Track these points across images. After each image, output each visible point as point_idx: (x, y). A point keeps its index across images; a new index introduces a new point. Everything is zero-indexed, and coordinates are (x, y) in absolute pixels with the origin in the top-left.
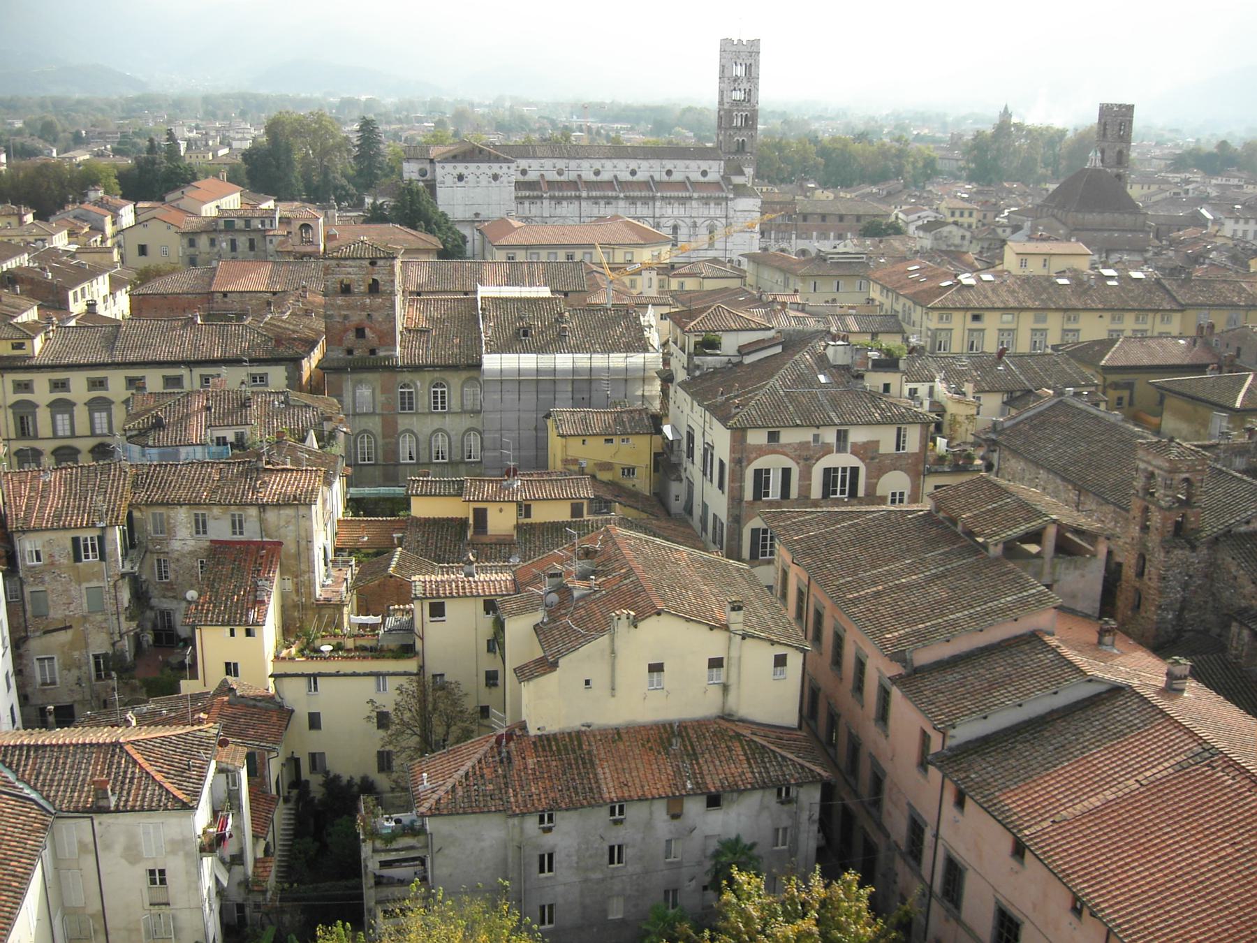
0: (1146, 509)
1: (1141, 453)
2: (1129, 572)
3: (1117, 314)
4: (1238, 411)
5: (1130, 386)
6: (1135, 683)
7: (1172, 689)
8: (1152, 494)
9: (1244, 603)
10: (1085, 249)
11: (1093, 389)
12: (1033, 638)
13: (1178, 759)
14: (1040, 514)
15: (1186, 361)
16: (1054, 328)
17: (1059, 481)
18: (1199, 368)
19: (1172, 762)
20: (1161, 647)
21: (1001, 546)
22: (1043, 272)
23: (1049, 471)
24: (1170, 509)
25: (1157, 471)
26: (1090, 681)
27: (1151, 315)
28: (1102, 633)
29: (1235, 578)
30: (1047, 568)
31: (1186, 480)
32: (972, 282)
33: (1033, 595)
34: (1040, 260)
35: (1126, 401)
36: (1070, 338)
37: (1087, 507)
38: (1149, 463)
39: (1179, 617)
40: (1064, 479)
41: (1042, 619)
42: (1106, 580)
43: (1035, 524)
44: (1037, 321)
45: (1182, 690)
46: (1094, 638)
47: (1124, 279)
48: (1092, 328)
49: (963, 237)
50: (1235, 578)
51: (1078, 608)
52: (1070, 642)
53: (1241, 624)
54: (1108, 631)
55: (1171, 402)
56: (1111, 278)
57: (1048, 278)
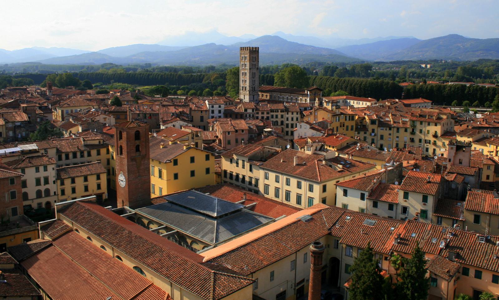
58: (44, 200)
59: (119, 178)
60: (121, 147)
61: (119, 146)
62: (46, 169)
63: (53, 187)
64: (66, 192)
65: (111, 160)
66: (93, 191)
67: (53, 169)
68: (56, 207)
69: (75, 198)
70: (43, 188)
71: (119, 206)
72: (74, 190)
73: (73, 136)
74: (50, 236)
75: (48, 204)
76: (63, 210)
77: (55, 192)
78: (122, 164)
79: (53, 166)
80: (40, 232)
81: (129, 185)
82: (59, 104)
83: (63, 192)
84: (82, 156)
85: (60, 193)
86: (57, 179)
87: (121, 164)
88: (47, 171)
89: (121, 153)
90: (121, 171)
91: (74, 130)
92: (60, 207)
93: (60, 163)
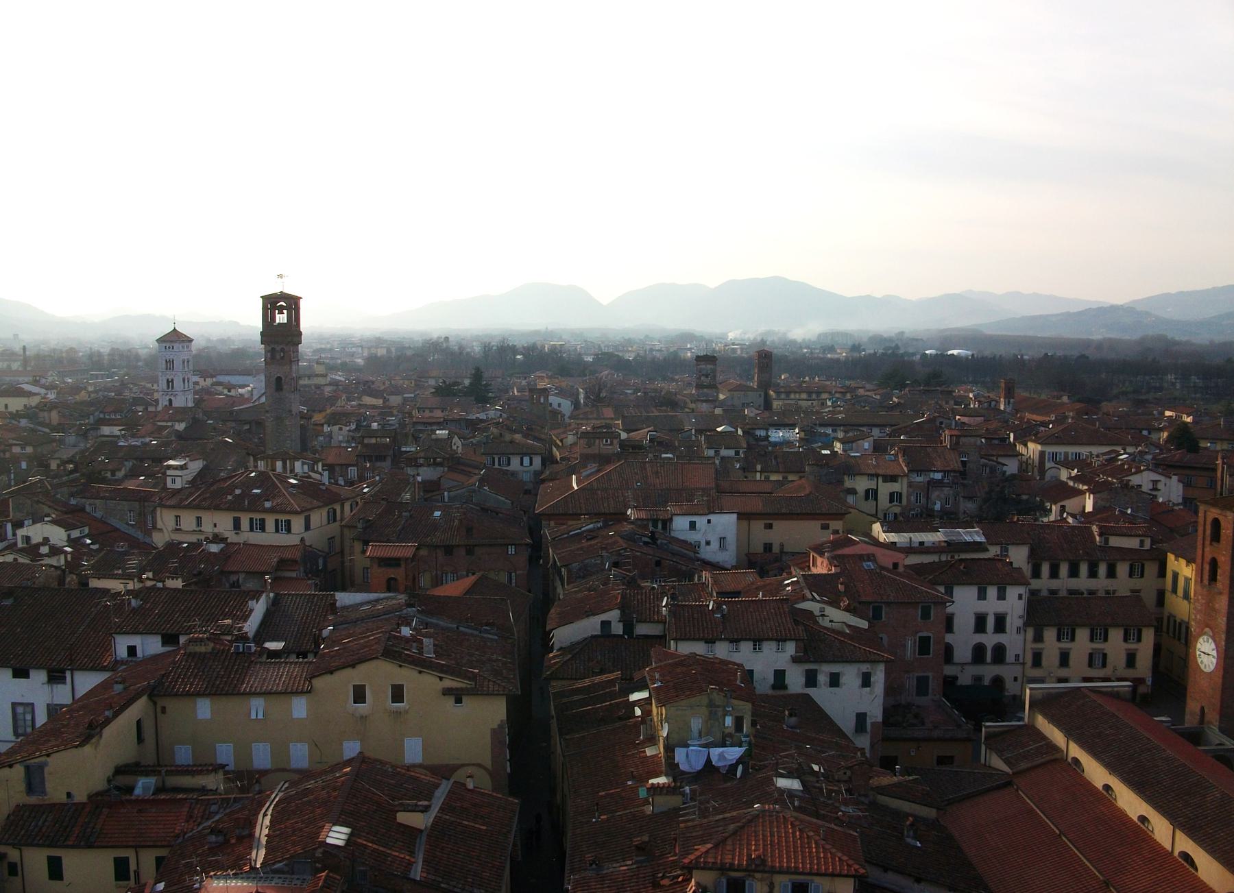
58: (989, 672)
59: (1199, 646)
60: (1214, 564)
61: (1208, 557)
62: (1001, 596)
63: (1015, 641)
64: (1044, 662)
65: (1169, 596)
66: (1115, 669)
67: (1020, 597)
68: (1028, 691)
69: (1065, 680)
70: (990, 639)
71: (1190, 721)
72: (1064, 659)
73: (1070, 520)
74: (1007, 762)
75: (998, 681)
76: (1044, 704)
77: (1017, 656)
78: (1214, 610)
79: (1021, 590)
80: (983, 747)
81: (1225, 669)
82: (1035, 435)
83: (1037, 660)
84: (1093, 574)
85: (1029, 659)
86: (1026, 625)
87: (1209, 609)
88: (1004, 599)
89: (1213, 578)
90: (1207, 626)
91: (1071, 504)
92: (1039, 694)
93: (1035, 584)
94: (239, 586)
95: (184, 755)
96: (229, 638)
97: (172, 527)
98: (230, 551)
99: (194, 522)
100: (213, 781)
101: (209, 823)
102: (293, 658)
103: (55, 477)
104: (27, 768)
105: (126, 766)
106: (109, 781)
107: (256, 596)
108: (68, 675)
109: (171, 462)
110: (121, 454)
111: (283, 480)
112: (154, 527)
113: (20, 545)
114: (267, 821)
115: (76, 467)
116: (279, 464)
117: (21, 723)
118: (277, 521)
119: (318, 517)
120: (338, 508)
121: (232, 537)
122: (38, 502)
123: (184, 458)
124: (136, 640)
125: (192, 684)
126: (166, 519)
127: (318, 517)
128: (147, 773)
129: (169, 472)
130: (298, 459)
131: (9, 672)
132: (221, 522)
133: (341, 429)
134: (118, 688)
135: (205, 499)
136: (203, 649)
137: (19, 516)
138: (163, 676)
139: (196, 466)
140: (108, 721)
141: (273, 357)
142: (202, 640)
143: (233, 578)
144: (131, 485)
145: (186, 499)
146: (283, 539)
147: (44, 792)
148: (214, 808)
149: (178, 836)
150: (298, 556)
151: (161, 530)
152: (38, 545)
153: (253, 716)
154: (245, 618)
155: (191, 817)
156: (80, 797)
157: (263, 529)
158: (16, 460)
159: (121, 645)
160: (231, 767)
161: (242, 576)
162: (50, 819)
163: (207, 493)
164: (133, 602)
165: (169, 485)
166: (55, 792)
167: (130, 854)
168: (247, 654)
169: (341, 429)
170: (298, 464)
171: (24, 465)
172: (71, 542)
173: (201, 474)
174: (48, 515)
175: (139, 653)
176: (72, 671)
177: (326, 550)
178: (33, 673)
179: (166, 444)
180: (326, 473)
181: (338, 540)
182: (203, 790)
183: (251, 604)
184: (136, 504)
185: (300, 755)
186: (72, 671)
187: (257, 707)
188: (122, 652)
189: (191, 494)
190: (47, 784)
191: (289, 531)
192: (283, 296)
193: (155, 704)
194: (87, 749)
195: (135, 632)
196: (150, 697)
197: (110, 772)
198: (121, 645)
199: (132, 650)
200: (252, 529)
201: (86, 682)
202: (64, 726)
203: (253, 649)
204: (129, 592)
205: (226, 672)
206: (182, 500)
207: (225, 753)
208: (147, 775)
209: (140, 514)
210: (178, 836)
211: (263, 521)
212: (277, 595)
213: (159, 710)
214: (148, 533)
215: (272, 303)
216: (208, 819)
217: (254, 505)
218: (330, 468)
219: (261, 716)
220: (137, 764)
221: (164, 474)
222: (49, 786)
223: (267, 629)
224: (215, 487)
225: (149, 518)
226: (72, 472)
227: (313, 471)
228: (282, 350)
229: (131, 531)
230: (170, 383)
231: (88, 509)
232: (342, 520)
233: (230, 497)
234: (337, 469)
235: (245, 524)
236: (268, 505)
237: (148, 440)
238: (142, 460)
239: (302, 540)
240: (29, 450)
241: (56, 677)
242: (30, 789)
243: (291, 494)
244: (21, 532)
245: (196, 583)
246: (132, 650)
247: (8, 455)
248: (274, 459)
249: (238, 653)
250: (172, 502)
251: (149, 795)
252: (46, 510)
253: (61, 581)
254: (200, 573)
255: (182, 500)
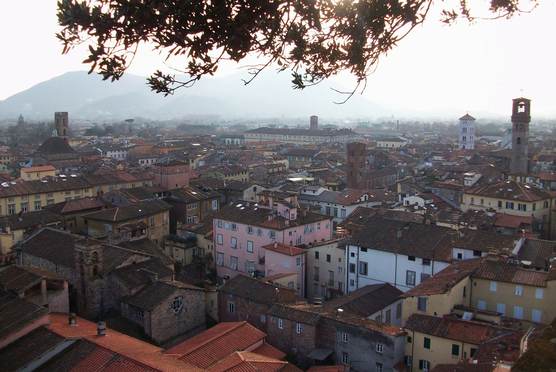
0: (82, 266)
1: (76, 245)
2: (80, 292)
3: (68, 192)
4: (115, 222)
5: (74, 219)
6: (85, 336)
7: (100, 334)
8: (83, 260)
9: (124, 295)
10: (53, 168)
11: (60, 222)
12: (43, 329)
13: (106, 362)
14: (38, 277)
15: (94, 206)
16: (44, 200)
17: (48, 261)
18: (99, 208)
19: (104, 364)
20: (96, 320)
21: (23, 294)
22: (38, 179)
23: (43, 258)
24: (90, 264)
25: (83, 251)
26: (67, 340)
27: (81, 191)
28: (70, 320)
29: (119, 286)
30: (45, 298)
31: (95, 252)
32: (7, 185)
33: (39, 311)
34: (36, 174)
35: (74, 224)
36: (51, 203)
37: (60, 270)
38: (79, 248)
39: (102, 305)
40: (49, 260)
41: (45, 320)
42: (70, 297)
43: (37, 282)
44: (36, 198)
45: (105, 334)
46: (68, 322)
47: (69, 178)
48: (59, 198)
49: (4, 168)
50: (119, 286)
51: (61, 311)
52: (58, 326)
53: (124, 302)
54: (73, 318)
55: (90, 222)
56: (64, 178)
57: (39, 181)
94: (501, 233)
95: (482, 305)
96: (507, 256)
97: (468, 203)
98: (497, 217)
99: (480, 201)
100: (497, 320)
101: (496, 338)
102: (534, 270)
103: (417, 176)
104: (419, 299)
105: (458, 305)
106: (451, 311)
107: (518, 239)
108: (431, 262)
109: (467, 174)
110: (443, 169)
111: (523, 186)
112: (462, 202)
113: (404, 204)
114: (526, 343)
115: (425, 173)
116: (518, 178)
117: (409, 279)
118: (519, 205)
119: (539, 205)
120: (549, 201)
121: (498, 211)
122: (412, 187)
123: (473, 172)
124: (462, 251)
125: (489, 275)
126: (467, 199)
127: (539, 205)
128: (468, 311)
129: (465, 178)
130: (528, 176)
131: (407, 257)
132: (493, 203)
133: (545, 163)
134: (456, 271)
135: (485, 192)
136: (494, 260)
137: (404, 192)
138: (476, 269)
139: (478, 176)
140: (453, 285)
141: (517, 128)
142: (494, 256)
143: (499, 229)
144: (447, 182)
145: (477, 191)
146: (521, 213)
147: (425, 310)
148: (499, 332)
149: (482, 341)
150: (530, 222)
151: (464, 203)
152: (413, 206)
153: (516, 294)
154: (513, 248)
155: (488, 334)
156: (440, 315)
157: (512, 208)
158: (399, 168)
159: (455, 252)
160: (503, 315)
161: (503, 228)
162: (427, 322)
163: (483, 188)
164: (461, 234)
165: (466, 184)
166: (430, 311)
167: (460, 344)
168: (514, 265)
169: (545, 163)
170: (528, 179)
171: (402, 171)
172: (427, 205)
173: (479, 181)
174: (417, 193)
175: (463, 257)
176: (433, 260)
177: (542, 220)
178: (416, 259)
179: (463, 166)
180: (541, 184)
181: (547, 217)
182: (492, 323)
183: (515, 242)
184: (454, 192)
185: (537, 316)
186: (433, 260)
187: (519, 290)
188: (455, 256)
189: (479, 189)
190: (427, 307)
191: (525, 210)
192: (523, 100)
193: (472, 280)
194: (445, 295)
195: (462, 248)
196: (471, 278)
197: (452, 307)
198: (455, 252)
199: (460, 256)
200: (507, 207)
201: (439, 267)
202: (434, 284)
203: (518, 263)
204: (460, 230)
205: (505, 271)
206: (475, 191)
207: (501, 308)
208: (468, 311)
209: (455, 196)
210: (482, 341)
211: (512, 204)
212: (526, 239)
213: (473, 284)
214: (459, 205)
215: (517, 103)
216: (496, 336)
217: (509, 196)
218: (542, 181)
219: (520, 294)
220: (462, 306)
221: (464, 179)
222: (428, 307)
223: (522, 254)
224: (490, 186)
225: (460, 198)
226: (423, 175)
227: (535, 182)
228: (521, 125)
229: (452, 204)
230: (464, 138)
231: (433, 191)
232: (551, 207)
233: (497, 192)
234: (546, 182)
235: (504, 205)
236: (515, 197)
237: (455, 163)
238: (453, 172)
239: (533, 215)
240: (405, 164)
241: (426, 262)
242: (419, 308)
243: (527, 193)
244: (405, 199)
245: (481, 229)
246: (460, 256)
247: (396, 166)
248: (516, 175)
249: (511, 264)
250: (469, 192)
251: (469, 320)
252: (416, 191)
253: (424, 221)
254: (484, 225)
255: (475, 191)
